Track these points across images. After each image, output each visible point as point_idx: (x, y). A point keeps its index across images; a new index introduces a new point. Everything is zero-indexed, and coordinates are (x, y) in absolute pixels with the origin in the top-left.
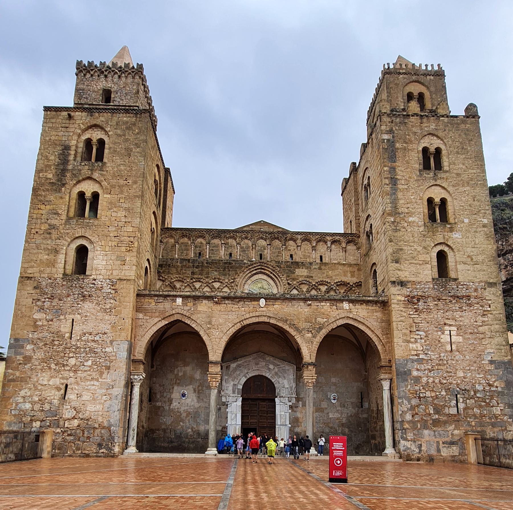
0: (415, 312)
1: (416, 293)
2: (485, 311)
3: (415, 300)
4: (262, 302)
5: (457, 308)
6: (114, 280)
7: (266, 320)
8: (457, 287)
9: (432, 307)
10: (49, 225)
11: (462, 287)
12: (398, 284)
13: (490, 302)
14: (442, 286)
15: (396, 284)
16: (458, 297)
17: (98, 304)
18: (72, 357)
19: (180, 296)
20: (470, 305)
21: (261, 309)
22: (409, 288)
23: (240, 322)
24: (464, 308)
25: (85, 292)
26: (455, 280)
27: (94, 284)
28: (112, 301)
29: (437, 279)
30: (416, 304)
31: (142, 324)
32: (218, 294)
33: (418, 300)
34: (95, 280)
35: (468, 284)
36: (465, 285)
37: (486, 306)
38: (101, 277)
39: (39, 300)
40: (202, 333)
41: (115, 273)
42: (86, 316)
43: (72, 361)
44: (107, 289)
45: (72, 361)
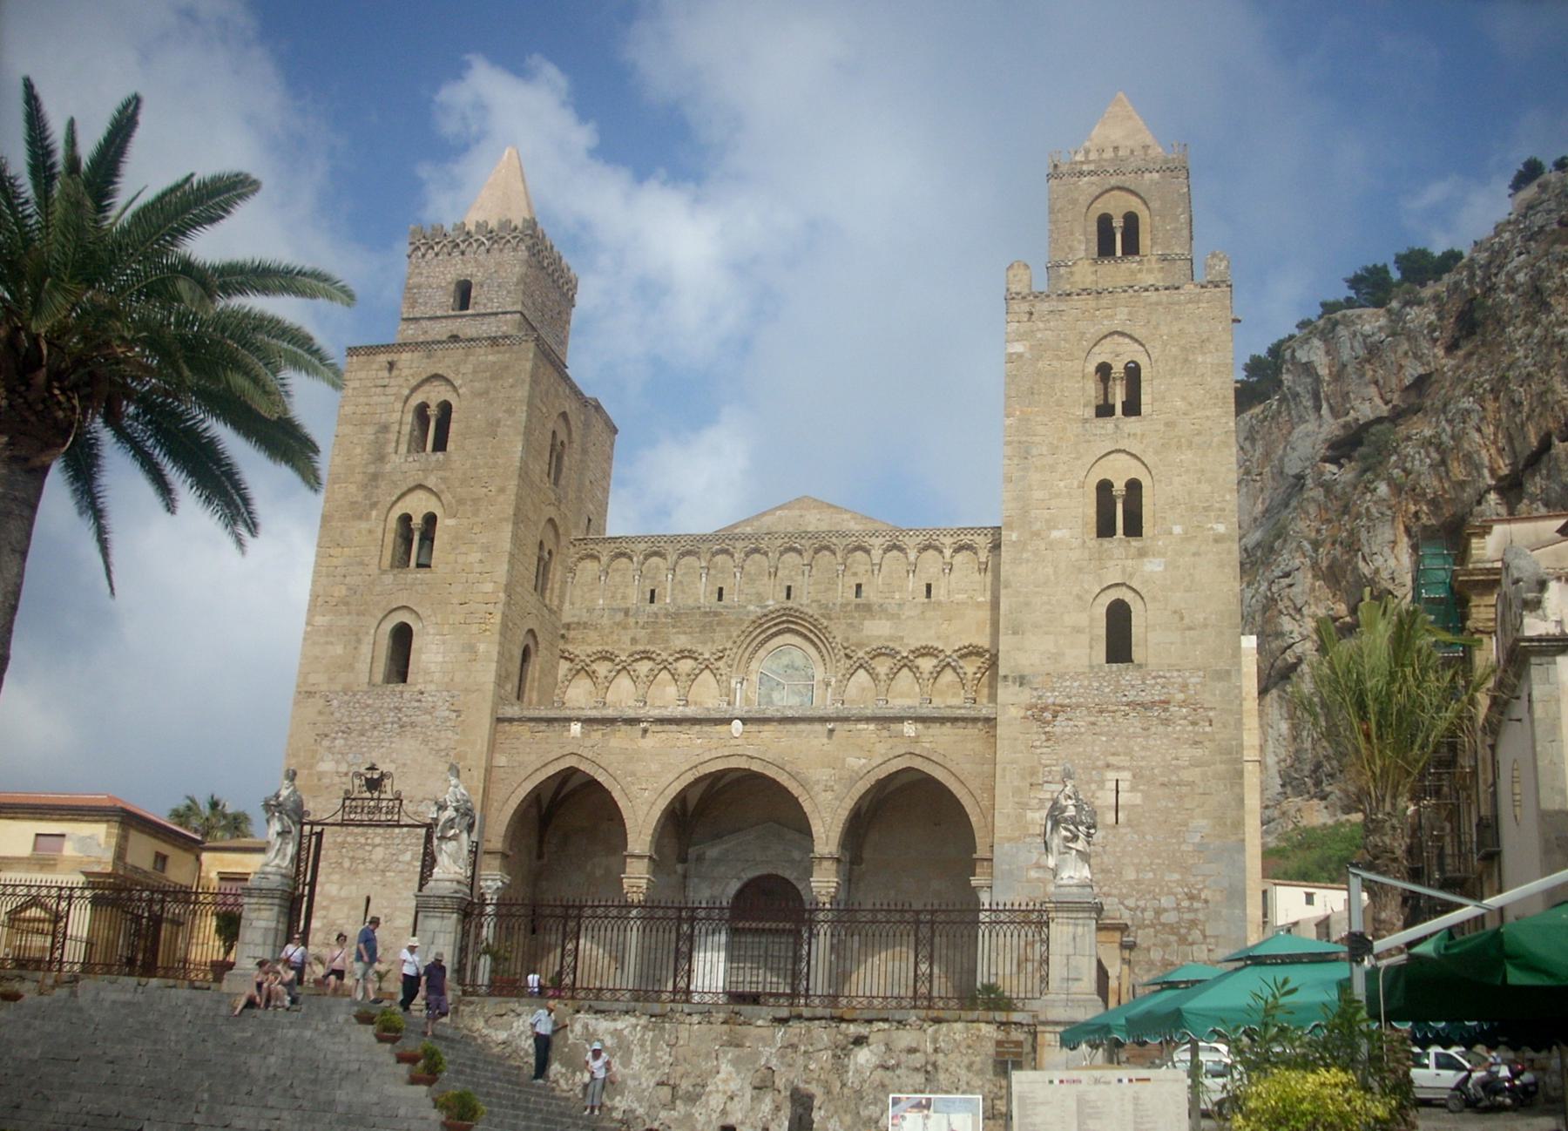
0: (1048, 740)
1: (1050, 700)
2: (1197, 733)
3: (1048, 715)
4: (737, 724)
5: (1138, 730)
6: (456, 693)
7: (743, 764)
8: (1144, 683)
9: (1083, 730)
10: (349, 589)
11: (1153, 682)
12: (1014, 682)
13: (1211, 714)
14: (1109, 681)
15: (1010, 679)
16: (1142, 705)
17: (425, 742)
18: (379, 845)
19: (578, 720)
20: (1166, 722)
21: (733, 742)
22: (1036, 689)
23: (691, 769)
24: (1153, 729)
25: (404, 719)
26: (1140, 666)
27: (420, 701)
28: (450, 734)
29: (1100, 666)
30: (1048, 723)
31: (504, 776)
32: (651, 713)
33: (1055, 717)
34: (422, 693)
35: (1168, 675)
36: (1160, 677)
37: (1202, 723)
38: (432, 687)
39: (326, 736)
40: (616, 795)
41: (457, 679)
42: (405, 765)
43: (379, 853)
44: (443, 712)
45: (379, 853)
